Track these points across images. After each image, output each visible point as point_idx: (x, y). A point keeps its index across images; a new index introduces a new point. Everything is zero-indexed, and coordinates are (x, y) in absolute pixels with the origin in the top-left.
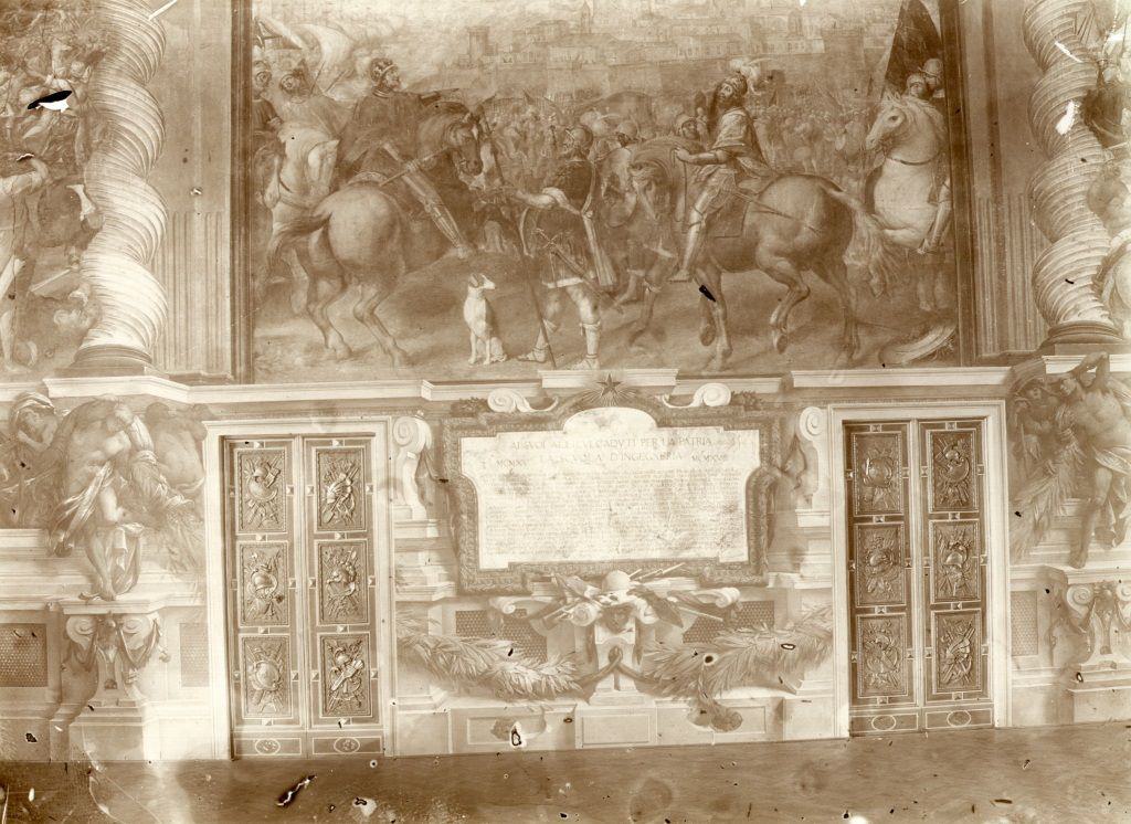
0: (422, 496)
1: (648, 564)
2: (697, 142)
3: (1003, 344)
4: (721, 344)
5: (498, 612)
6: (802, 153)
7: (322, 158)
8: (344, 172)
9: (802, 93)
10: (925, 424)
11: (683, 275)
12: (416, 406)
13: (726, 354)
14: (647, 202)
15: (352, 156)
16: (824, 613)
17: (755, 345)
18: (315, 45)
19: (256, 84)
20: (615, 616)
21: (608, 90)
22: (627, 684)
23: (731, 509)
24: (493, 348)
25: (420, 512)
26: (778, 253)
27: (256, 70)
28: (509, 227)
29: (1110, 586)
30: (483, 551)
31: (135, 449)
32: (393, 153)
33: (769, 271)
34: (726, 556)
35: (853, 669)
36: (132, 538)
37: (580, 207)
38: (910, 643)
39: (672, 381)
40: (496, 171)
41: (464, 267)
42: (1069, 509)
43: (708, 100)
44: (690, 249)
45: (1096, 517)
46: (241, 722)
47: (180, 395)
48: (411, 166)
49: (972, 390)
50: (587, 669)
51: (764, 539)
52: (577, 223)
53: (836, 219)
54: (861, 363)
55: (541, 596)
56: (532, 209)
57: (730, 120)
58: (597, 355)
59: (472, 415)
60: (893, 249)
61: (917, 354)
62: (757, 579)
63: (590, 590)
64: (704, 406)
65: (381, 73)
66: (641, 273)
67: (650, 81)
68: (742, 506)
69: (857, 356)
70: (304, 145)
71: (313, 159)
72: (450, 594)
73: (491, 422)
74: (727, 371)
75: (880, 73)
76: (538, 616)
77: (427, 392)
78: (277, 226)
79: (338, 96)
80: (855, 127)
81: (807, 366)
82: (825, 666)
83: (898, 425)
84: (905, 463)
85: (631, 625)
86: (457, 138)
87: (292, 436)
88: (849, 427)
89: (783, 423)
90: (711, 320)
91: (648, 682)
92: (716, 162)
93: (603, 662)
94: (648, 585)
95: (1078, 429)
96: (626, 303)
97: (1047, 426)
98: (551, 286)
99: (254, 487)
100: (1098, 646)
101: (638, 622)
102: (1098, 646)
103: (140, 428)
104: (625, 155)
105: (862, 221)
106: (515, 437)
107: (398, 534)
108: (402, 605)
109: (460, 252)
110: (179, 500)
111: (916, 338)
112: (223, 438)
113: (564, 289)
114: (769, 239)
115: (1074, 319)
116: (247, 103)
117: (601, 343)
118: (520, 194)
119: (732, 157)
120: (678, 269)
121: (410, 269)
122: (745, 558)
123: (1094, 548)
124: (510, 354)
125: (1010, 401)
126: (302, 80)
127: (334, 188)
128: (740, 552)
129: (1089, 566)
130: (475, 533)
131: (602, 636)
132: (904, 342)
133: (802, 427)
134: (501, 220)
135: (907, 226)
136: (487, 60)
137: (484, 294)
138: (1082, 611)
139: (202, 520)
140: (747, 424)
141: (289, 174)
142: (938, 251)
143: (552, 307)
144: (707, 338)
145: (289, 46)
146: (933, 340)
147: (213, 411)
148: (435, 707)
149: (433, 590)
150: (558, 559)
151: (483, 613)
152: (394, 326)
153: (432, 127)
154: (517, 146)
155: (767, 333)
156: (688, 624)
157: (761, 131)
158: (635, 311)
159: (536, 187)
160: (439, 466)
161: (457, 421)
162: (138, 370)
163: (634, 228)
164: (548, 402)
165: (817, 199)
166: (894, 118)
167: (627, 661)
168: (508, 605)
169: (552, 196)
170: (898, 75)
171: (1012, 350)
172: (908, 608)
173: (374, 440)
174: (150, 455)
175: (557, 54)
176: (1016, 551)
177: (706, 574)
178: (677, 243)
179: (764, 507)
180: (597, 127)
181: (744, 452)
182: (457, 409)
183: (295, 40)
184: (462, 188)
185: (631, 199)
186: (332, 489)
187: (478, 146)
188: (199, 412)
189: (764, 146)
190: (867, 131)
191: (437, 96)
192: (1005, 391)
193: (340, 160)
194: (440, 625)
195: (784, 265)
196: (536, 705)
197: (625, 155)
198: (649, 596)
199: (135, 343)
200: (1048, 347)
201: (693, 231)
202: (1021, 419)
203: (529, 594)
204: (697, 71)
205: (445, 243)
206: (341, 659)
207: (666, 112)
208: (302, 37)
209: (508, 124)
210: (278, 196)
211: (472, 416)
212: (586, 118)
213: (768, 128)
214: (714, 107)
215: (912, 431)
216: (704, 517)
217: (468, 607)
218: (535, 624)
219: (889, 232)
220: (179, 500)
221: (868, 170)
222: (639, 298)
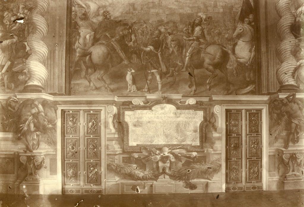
0: (114, 126)
3: (268, 90)
4: (194, 88)
5: (134, 157)
7: (90, 37)
8: (95, 41)
10: (247, 110)
11: (184, 69)
12: (113, 103)
13: (195, 91)
15: (98, 36)
16: (219, 160)
17: (203, 89)
18: (89, 7)
19: (73, 17)
21: (166, 20)
24: (134, 88)
25: (113, 130)
26: (209, 64)
27: (73, 13)
28: (139, 57)
29: (295, 154)
32: (109, 36)
33: (207, 69)
34: (194, 144)
36: (37, 136)
37: (157, 51)
38: (242, 168)
39: (181, 98)
41: (127, 66)
42: (284, 134)
43: (192, 24)
46: (65, 185)
47: (50, 98)
48: (113, 39)
53: (225, 56)
54: (230, 94)
55: (145, 153)
56: (145, 51)
57: (197, 29)
58: (161, 90)
59: (128, 105)
60: (240, 64)
61: (245, 92)
62: (202, 150)
63: (158, 152)
65: (106, 15)
66: (173, 69)
67: (177, 18)
68: (198, 131)
69: (229, 92)
70: (85, 33)
71: (88, 37)
72: (121, 152)
73: (133, 107)
74: (195, 95)
75: (237, 18)
76: (144, 158)
77: (116, 99)
78: (78, 54)
79: (94, 20)
80: (230, 32)
81: (216, 94)
82: (219, 174)
83: (240, 111)
84: (242, 120)
85: (168, 161)
86: (126, 32)
87: (81, 110)
88: (227, 111)
89: (210, 109)
90: (191, 82)
92: (194, 40)
94: (173, 151)
95: (287, 112)
98: (149, 72)
99: (70, 123)
100: (291, 170)
102: (291, 170)
103: (40, 107)
104: (170, 38)
105: (232, 57)
106: (139, 111)
107: (107, 136)
108: (108, 155)
109: (126, 62)
110: (50, 126)
112: (62, 110)
114: (207, 61)
115: (287, 83)
116: (71, 22)
117: (162, 87)
119: (198, 39)
120: (183, 68)
121: (112, 66)
122: (199, 144)
123: (291, 144)
124: (138, 89)
125: (269, 104)
126: (85, 17)
127: (93, 45)
129: (289, 149)
134: (136, 53)
135: (243, 58)
136: (134, 12)
137: (132, 73)
138: (287, 160)
139: (56, 131)
140: (200, 109)
141: (81, 41)
142: (251, 65)
143: (150, 77)
145: (82, 7)
146: (249, 88)
147: (60, 103)
149: (117, 151)
150: (149, 144)
151: (129, 158)
152: (108, 81)
155: (206, 85)
156: (183, 162)
157: (206, 32)
158: (170, 79)
159: (146, 46)
163: (172, 57)
164: (148, 102)
165: (220, 51)
166: (241, 30)
167: (167, 171)
168: (136, 155)
169: (150, 48)
170: (242, 19)
171: (270, 91)
173: (102, 111)
174: (43, 114)
175: (152, 11)
176: (270, 144)
178: (183, 61)
180: (163, 30)
181: (199, 117)
182: (124, 104)
183: (84, 5)
184: (127, 45)
185: (171, 49)
186: (90, 124)
187: (131, 34)
188: (56, 103)
189: (206, 36)
190: (234, 33)
191: (121, 21)
192: (268, 102)
193: (95, 38)
195: (211, 67)
197: (170, 38)
198: (173, 154)
199: (40, 84)
200: (280, 91)
201: (187, 58)
202: (272, 110)
203: (142, 152)
204: (189, 16)
205: (122, 60)
209: (139, 29)
210: (78, 45)
211: (128, 106)
213: (207, 31)
214: (193, 26)
215: (243, 111)
218: (143, 161)
219: (239, 59)
220: (50, 126)
221: (233, 43)
222: (172, 76)
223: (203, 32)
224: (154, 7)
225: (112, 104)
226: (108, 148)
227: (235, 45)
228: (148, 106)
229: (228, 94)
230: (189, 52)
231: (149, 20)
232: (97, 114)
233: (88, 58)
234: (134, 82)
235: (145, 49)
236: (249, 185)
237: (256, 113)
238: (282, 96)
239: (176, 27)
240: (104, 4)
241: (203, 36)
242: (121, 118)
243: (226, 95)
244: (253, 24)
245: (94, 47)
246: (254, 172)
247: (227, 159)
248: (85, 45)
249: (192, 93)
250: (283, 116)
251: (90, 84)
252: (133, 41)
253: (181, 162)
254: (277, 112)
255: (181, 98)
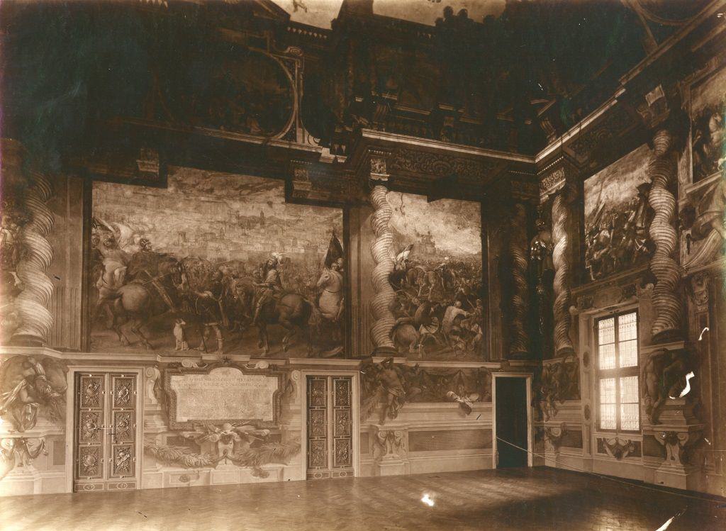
0: (156, 395)
1: (237, 421)
2: (259, 280)
3: (359, 352)
4: (265, 349)
5: (183, 437)
6: (295, 286)
7: (120, 272)
8: (128, 278)
9: (296, 266)
10: (333, 378)
13: (267, 351)
14: (242, 299)
15: (132, 273)
16: (298, 438)
17: (278, 349)
18: (118, 230)
19: (93, 242)
20: (226, 439)
21: (229, 258)
22: (229, 462)
23: (267, 403)
24: (184, 345)
25: (154, 401)
27: (93, 237)
29: (393, 432)
30: (178, 415)
31: (37, 374)
35: (308, 457)
36: (32, 407)
37: (217, 299)
39: (248, 360)
40: (187, 283)
42: (379, 406)
43: (264, 266)
44: (256, 315)
45: (388, 409)
46: (78, 478)
47: (57, 355)
48: (155, 279)
49: (350, 367)
50: (215, 457)
51: (278, 413)
52: (218, 303)
53: (306, 309)
54: (312, 357)
55: (199, 431)
56: (201, 298)
57: (271, 273)
58: (222, 349)
59: (176, 368)
60: (325, 320)
61: (332, 355)
64: (259, 368)
65: (144, 243)
66: (239, 323)
68: (271, 402)
70: (112, 266)
71: (117, 272)
72: (165, 430)
74: (268, 357)
75: (323, 262)
76: (199, 438)
77: (159, 359)
78: (101, 296)
79: (127, 250)
80: (313, 279)
81: (293, 356)
82: (298, 456)
83: (325, 377)
84: (327, 390)
86: (173, 270)
87: (106, 373)
89: (286, 375)
91: (236, 462)
92: (266, 287)
93: (221, 454)
95: (383, 381)
96: (233, 332)
97: (373, 379)
99: (88, 391)
100: (388, 451)
101: (234, 441)
102: (388, 451)
103: (40, 367)
104: (235, 282)
105: (315, 310)
106: (192, 376)
107: (146, 409)
108: (146, 434)
109: (173, 310)
110: (56, 394)
111: (331, 350)
112: (75, 373)
113: (211, 326)
114: (284, 314)
116: (89, 249)
117: (223, 346)
118: (196, 292)
119: (271, 285)
121: (154, 315)
122: (272, 420)
123: (387, 419)
124: (190, 347)
126: (113, 243)
127: (124, 284)
128: (270, 417)
129: (385, 425)
130: (175, 409)
131: (221, 446)
132: (328, 350)
133: (292, 376)
135: (329, 313)
136: (185, 244)
137: (181, 326)
139: (66, 402)
141: (107, 276)
143: (207, 332)
144: (261, 346)
145: (107, 229)
146: (336, 350)
147: (72, 362)
148: (157, 471)
149: (159, 429)
150: (206, 419)
151: (178, 438)
152: (147, 335)
153: (164, 265)
154: (195, 274)
156: (251, 442)
157: (282, 278)
159: (202, 290)
160: (163, 386)
161: (169, 370)
162: (41, 345)
164: (204, 365)
166: (327, 277)
167: (230, 454)
168: (187, 434)
169: (207, 294)
170: (328, 264)
172: (327, 438)
173: (138, 376)
175: (211, 244)
176: (362, 419)
177: (256, 424)
178: (251, 312)
179: (278, 403)
180: (225, 270)
181: (273, 384)
182: (170, 365)
183: (112, 229)
186: (120, 393)
187: (181, 274)
188: (66, 362)
189: (283, 283)
190: (318, 280)
191: (166, 255)
194: (161, 441)
195: (287, 323)
196: (196, 470)
197: (235, 282)
198: (238, 432)
199: (39, 335)
200: (374, 354)
201: (257, 310)
203: (195, 431)
204: (261, 256)
206: (121, 454)
207: (249, 269)
208: (113, 227)
210: (102, 283)
211: (177, 369)
212: (221, 268)
213: (284, 276)
216: (258, 405)
217: (170, 435)
220: (56, 394)
223: (278, 277)
224: (214, 239)
225: (154, 366)
226: (145, 425)
227: (320, 295)
228: (204, 368)
229: (310, 357)
230: (259, 301)
231: (207, 257)
232: (130, 379)
233: (117, 301)
234: (185, 338)
235: (200, 294)
236: (336, 470)
237: (344, 382)
238: (377, 360)
239: (244, 269)
240: (140, 229)
241: (278, 282)
242: (166, 384)
243: (307, 357)
244: (342, 270)
245: (126, 286)
246: (342, 453)
247: (309, 438)
248: (113, 282)
249: (264, 354)
250: (378, 385)
251: (120, 338)
252: (183, 282)
253: (248, 441)
254: (370, 380)
255: (248, 360)
